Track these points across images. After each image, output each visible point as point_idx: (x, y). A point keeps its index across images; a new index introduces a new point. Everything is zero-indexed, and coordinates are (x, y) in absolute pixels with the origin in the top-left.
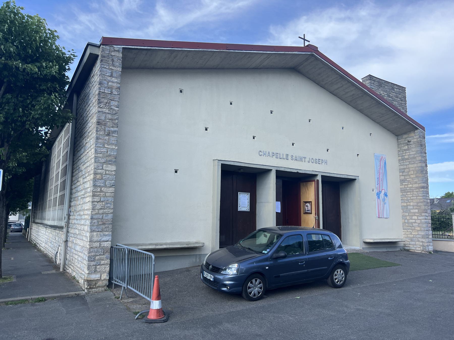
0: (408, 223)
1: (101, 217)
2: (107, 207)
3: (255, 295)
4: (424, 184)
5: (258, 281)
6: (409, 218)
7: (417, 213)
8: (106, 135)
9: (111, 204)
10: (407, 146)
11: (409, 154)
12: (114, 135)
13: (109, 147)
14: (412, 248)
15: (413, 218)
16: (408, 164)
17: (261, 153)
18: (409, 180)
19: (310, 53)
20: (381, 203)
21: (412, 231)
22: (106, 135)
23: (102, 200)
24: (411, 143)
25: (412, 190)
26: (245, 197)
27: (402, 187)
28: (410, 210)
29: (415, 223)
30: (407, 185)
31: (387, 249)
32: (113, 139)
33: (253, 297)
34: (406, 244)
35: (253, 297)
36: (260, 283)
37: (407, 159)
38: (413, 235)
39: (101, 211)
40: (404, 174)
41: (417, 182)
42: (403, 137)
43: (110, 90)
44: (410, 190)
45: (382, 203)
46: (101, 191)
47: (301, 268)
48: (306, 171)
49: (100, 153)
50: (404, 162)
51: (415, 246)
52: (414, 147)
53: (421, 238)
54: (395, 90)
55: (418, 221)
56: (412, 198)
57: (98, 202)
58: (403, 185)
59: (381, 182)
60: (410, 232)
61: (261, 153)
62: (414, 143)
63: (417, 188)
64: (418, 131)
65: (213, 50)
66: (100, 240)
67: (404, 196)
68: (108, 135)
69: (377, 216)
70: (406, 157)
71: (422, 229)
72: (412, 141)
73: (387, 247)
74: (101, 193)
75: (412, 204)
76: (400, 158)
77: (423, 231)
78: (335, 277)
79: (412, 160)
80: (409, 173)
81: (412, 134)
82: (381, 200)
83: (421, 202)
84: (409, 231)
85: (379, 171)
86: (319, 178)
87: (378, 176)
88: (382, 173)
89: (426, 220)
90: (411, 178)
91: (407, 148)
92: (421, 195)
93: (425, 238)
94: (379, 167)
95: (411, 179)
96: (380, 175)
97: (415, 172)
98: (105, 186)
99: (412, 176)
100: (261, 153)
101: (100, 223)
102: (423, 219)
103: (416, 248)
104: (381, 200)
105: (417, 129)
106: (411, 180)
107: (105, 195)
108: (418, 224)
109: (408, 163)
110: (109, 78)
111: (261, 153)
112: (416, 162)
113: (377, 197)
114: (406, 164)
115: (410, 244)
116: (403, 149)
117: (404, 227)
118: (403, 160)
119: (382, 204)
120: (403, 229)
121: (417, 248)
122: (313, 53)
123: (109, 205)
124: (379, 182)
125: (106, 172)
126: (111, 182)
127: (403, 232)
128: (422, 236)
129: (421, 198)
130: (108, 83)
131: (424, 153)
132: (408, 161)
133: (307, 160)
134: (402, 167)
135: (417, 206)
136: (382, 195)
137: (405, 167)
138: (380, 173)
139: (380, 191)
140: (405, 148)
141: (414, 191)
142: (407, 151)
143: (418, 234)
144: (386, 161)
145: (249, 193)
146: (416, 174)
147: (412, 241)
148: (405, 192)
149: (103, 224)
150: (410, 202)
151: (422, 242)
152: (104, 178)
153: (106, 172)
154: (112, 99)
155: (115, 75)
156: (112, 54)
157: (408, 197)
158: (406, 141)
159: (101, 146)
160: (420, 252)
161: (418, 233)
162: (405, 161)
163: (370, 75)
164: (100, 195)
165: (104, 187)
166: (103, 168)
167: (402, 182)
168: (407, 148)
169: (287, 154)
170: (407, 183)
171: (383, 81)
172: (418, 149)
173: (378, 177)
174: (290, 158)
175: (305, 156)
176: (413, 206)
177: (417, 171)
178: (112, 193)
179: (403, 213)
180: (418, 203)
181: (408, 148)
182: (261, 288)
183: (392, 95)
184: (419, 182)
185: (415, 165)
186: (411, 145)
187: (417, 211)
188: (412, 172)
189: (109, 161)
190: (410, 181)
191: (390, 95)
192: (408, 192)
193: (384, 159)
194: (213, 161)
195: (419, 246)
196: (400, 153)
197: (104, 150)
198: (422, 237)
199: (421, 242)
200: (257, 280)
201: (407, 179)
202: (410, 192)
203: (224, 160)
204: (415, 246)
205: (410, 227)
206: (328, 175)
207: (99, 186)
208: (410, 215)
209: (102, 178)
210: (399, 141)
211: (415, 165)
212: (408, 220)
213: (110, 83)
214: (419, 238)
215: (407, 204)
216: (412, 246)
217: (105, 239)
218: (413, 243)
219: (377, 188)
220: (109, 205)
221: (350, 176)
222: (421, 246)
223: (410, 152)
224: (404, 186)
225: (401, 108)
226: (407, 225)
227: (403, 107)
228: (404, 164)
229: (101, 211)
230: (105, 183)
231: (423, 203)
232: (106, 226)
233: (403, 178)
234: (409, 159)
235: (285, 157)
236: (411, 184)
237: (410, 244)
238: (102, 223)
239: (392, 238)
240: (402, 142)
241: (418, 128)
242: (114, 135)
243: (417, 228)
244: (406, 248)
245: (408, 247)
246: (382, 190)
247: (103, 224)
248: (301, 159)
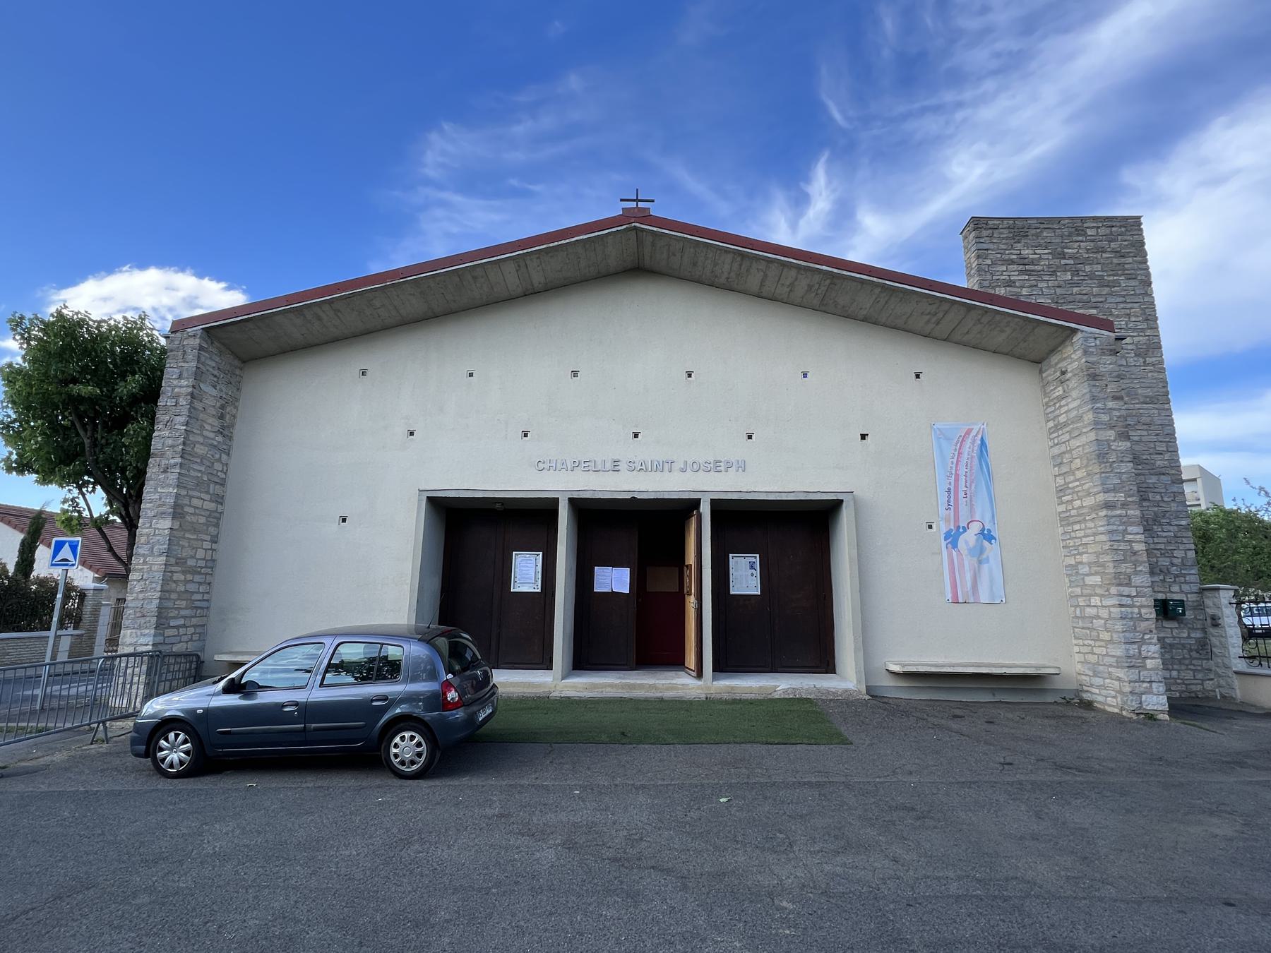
0: (1083, 618)
1: (140, 605)
2: (151, 589)
3: (171, 766)
4: (1113, 494)
5: (182, 737)
6: (1083, 604)
7: (1100, 586)
8: (162, 472)
9: (157, 583)
10: (1060, 388)
11: (1066, 408)
12: (172, 470)
13: (163, 491)
14: (1096, 696)
15: (1092, 604)
16: (1068, 438)
17: (542, 466)
18: (1074, 488)
19: (625, 227)
20: (963, 560)
21: (1093, 642)
22: (162, 472)
23: (144, 577)
24: (1069, 375)
25: (1082, 518)
26: (529, 562)
27: (1062, 508)
28: (1083, 579)
29: (1098, 617)
30: (1072, 501)
31: (994, 695)
32: (172, 477)
33: (169, 770)
34: (1084, 682)
35: (169, 770)
36: (185, 742)
37: (1066, 424)
38: (1097, 656)
39: (141, 596)
40: (1064, 469)
41: (1091, 491)
42: (1052, 364)
43: (174, 400)
44: (1079, 515)
45: (969, 562)
46: (145, 563)
47: (289, 718)
48: (658, 493)
49: (151, 502)
50: (1059, 436)
51: (1105, 691)
52: (1076, 385)
53: (1114, 667)
54: (1089, 232)
55: (1104, 613)
56: (1085, 540)
57: (139, 581)
58: (1063, 503)
59: (962, 501)
60: (1090, 645)
61: (541, 466)
62: (1074, 375)
63: (1094, 509)
64: (1079, 335)
65: (369, 288)
66: (136, 642)
67: (1068, 537)
68: (165, 471)
69: (949, 596)
70: (1062, 419)
71: (1115, 636)
72: (1069, 370)
73: (993, 691)
74: (145, 567)
75: (1085, 558)
76: (1051, 424)
77: (1116, 645)
78: (394, 751)
79: (1075, 426)
80: (1074, 466)
81: (1068, 350)
82: (964, 552)
83: (1105, 553)
84: (1086, 642)
85: (954, 472)
86: (705, 509)
87: (950, 483)
88: (966, 476)
89: (1123, 609)
90: (1078, 480)
91: (1061, 393)
92: (1102, 529)
93: (1122, 667)
94: (955, 461)
95: (1078, 483)
96: (957, 480)
97: (1085, 462)
98: (152, 554)
99: (1079, 474)
100: (541, 466)
101: (138, 615)
102: (1113, 606)
103: (1106, 697)
104: (964, 552)
105: (1075, 331)
106: (1077, 486)
107: (151, 568)
108: (1103, 621)
109: (1067, 437)
110: (175, 382)
111: (542, 466)
112: (1084, 430)
113: (947, 544)
114: (1063, 440)
115: (1092, 686)
116: (1055, 395)
117: (1076, 630)
118: (1057, 428)
119: (966, 563)
120: (1076, 638)
121: (1108, 697)
122: (633, 224)
123: (154, 585)
124: (952, 499)
125: (155, 532)
126: (161, 547)
127: (1076, 645)
128: (1115, 659)
129: (1104, 538)
130: (173, 390)
131: (1110, 399)
132: (1068, 429)
133: (676, 467)
134: (1056, 451)
135: (1097, 564)
136: (969, 538)
137: (1063, 448)
138: (957, 476)
139: (959, 527)
140: (1057, 394)
141: (1087, 518)
142: (1063, 403)
143: (1107, 655)
144: (984, 438)
145: (541, 553)
146: (1087, 466)
147: (1096, 674)
148: (1068, 525)
149: (141, 617)
150: (1081, 554)
151: (1119, 679)
152: (151, 541)
153: (155, 532)
154: (176, 414)
155: (185, 374)
156: (185, 343)
157: (1076, 538)
158: (1058, 374)
159: (152, 490)
160: (1116, 710)
161: (1108, 650)
162: (1060, 432)
163: (972, 217)
164: (143, 568)
165: (150, 556)
166: (151, 526)
167: (1061, 494)
168: (1061, 393)
169: (616, 458)
170: (1069, 498)
171: (1029, 222)
172: (1085, 391)
173: (949, 489)
174: (623, 466)
175: (670, 459)
176: (1089, 564)
177: (1088, 455)
178: (161, 565)
179: (1070, 586)
180: (1098, 554)
181: (1064, 391)
182: (187, 753)
183: (1075, 251)
184: (1095, 490)
185: (1083, 439)
186: (1068, 383)
187: (1098, 579)
188: (1078, 460)
189: (162, 513)
190: (1076, 490)
191: (1066, 251)
192: (1076, 523)
193: (980, 436)
194: (418, 492)
195: (1113, 693)
196: (1049, 410)
197: (156, 496)
198: (1117, 662)
199: (1115, 680)
200: (180, 734)
201: (1070, 485)
202: (1079, 522)
203: (433, 489)
204: (1104, 692)
205: (1088, 632)
206: (735, 497)
207: (143, 555)
208: (1085, 592)
209: (148, 542)
210: (1044, 375)
211: (1083, 439)
212: (1082, 608)
213: (176, 390)
214: (1110, 666)
215: (1077, 560)
216: (1097, 691)
217: (142, 640)
218: (1098, 681)
219: (947, 520)
220: (154, 585)
221: (819, 494)
222: (1117, 692)
223: (1070, 402)
224: (1065, 505)
225: (1123, 277)
226: (1081, 624)
227: (1126, 272)
228: (1061, 440)
229: (141, 596)
230: (153, 549)
231: (1108, 554)
232: (148, 619)
233: (1060, 481)
234: (1069, 422)
235: (609, 466)
236: (1078, 499)
237: (1092, 686)
238: (141, 615)
239: (986, 661)
240: (1050, 378)
241: (1078, 329)
242: (172, 470)
243: (1103, 633)
244: (1085, 696)
245: (1089, 695)
246: (969, 523)
247: (141, 617)
248: (659, 467)
